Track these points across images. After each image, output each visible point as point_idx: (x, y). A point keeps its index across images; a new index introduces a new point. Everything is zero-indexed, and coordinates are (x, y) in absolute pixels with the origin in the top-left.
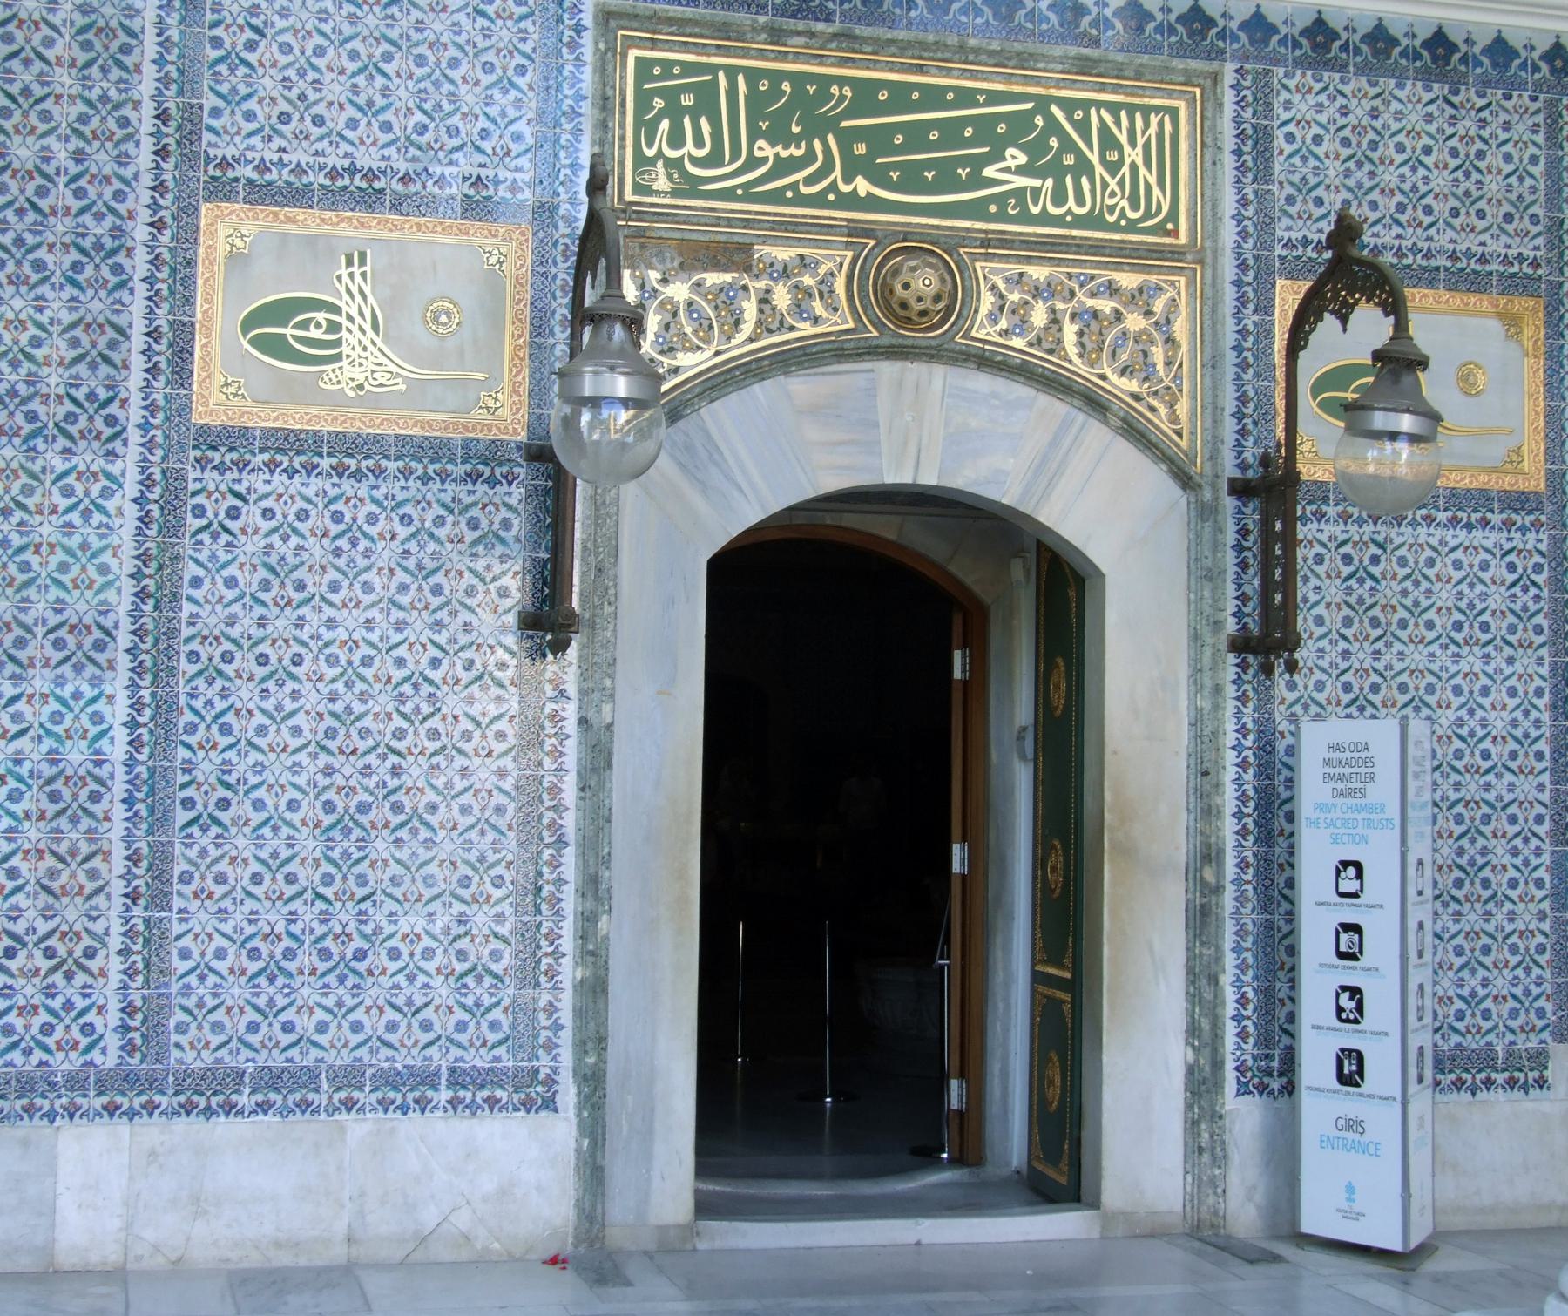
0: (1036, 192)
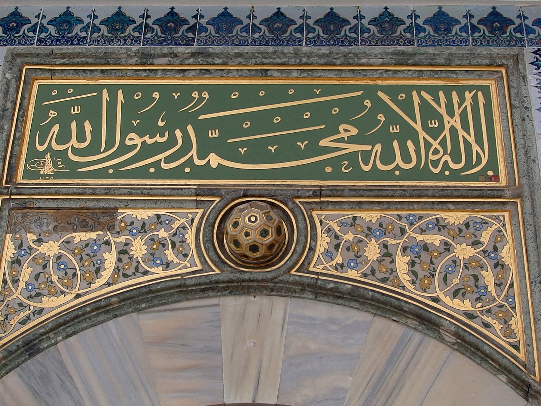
0: (366, 156)
